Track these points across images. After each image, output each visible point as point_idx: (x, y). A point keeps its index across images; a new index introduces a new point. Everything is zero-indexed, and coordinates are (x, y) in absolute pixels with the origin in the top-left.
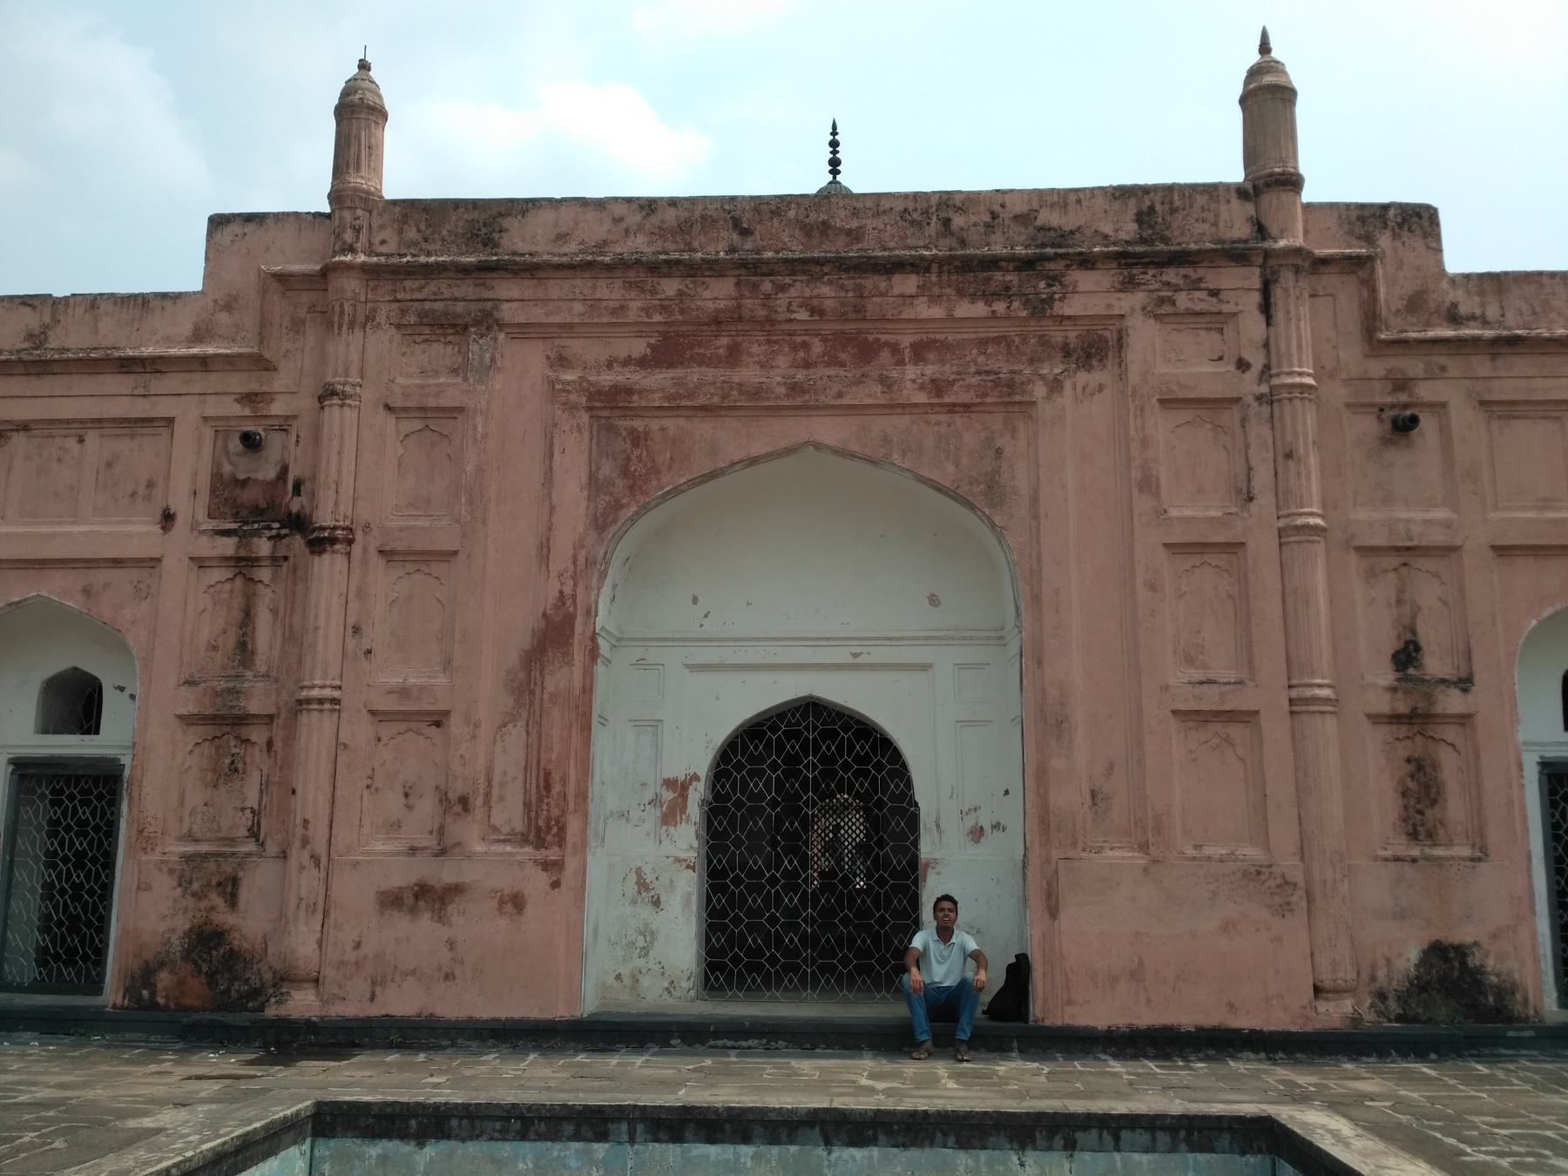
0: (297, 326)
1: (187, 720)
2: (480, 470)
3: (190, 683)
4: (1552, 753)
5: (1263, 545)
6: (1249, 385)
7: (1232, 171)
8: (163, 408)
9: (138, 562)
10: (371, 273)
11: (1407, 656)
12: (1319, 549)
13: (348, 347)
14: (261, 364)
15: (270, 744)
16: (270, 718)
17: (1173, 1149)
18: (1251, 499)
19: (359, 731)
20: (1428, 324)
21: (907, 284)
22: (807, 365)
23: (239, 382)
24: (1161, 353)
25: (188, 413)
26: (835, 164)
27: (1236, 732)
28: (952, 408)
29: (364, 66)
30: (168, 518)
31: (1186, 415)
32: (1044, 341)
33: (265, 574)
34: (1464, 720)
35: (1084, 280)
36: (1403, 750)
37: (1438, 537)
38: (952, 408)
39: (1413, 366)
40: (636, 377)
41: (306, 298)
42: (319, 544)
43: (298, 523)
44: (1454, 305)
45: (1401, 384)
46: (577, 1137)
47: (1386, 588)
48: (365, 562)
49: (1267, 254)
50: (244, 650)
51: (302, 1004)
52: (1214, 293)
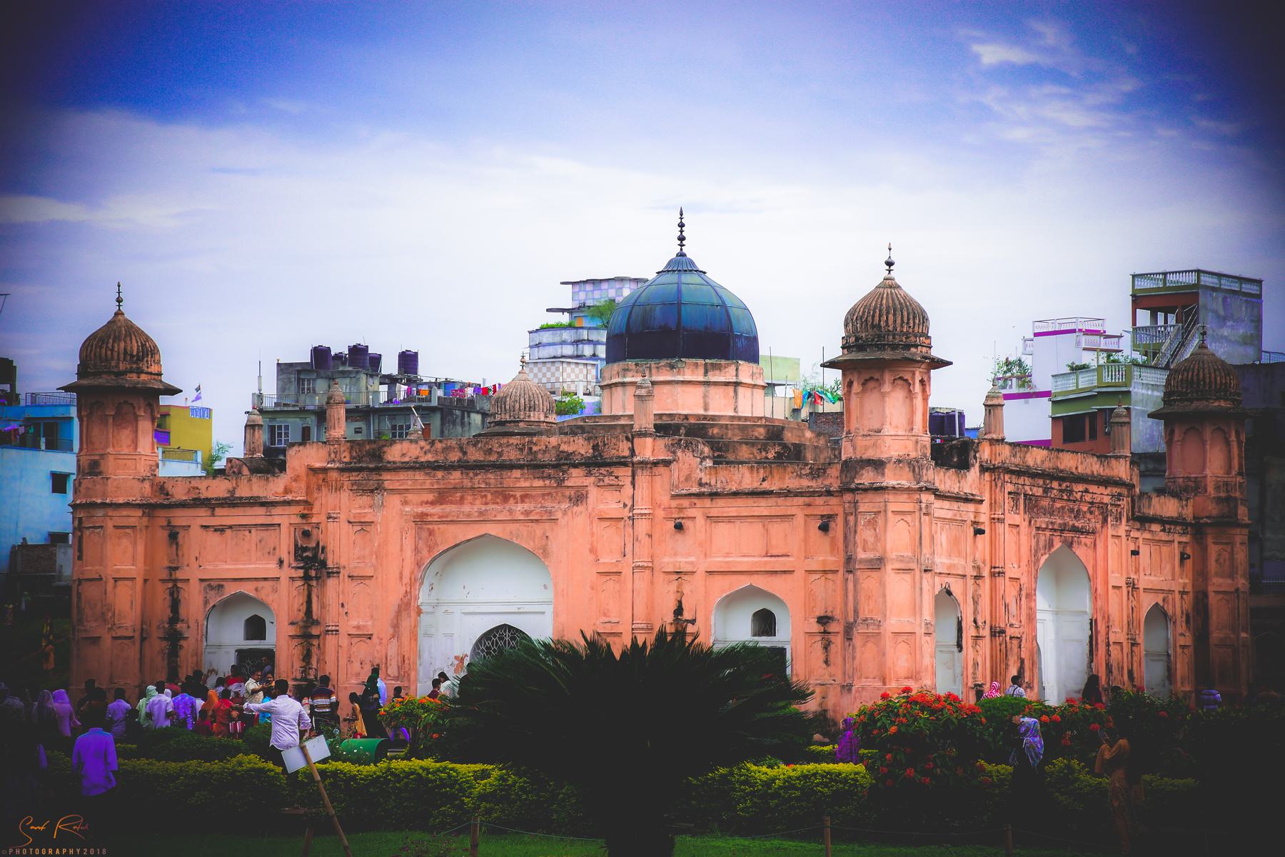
0: (319, 488)
1: (292, 637)
3: (292, 624)
5: (627, 572)
6: (626, 513)
8: (276, 520)
9: (273, 579)
10: (341, 470)
11: (679, 611)
16: (318, 637)
19: (344, 641)
25: (284, 521)
26: (682, 239)
28: (532, 521)
30: (281, 562)
31: (607, 523)
33: (314, 583)
35: (574, 472)
38: (532, 521)
39: (685, 502)
40: (430, 510)
41: (321, 476)
42: (329, 575)
43: (323, 564)
45: (681, 509)
47: (673, 587)
50: (309, 611)
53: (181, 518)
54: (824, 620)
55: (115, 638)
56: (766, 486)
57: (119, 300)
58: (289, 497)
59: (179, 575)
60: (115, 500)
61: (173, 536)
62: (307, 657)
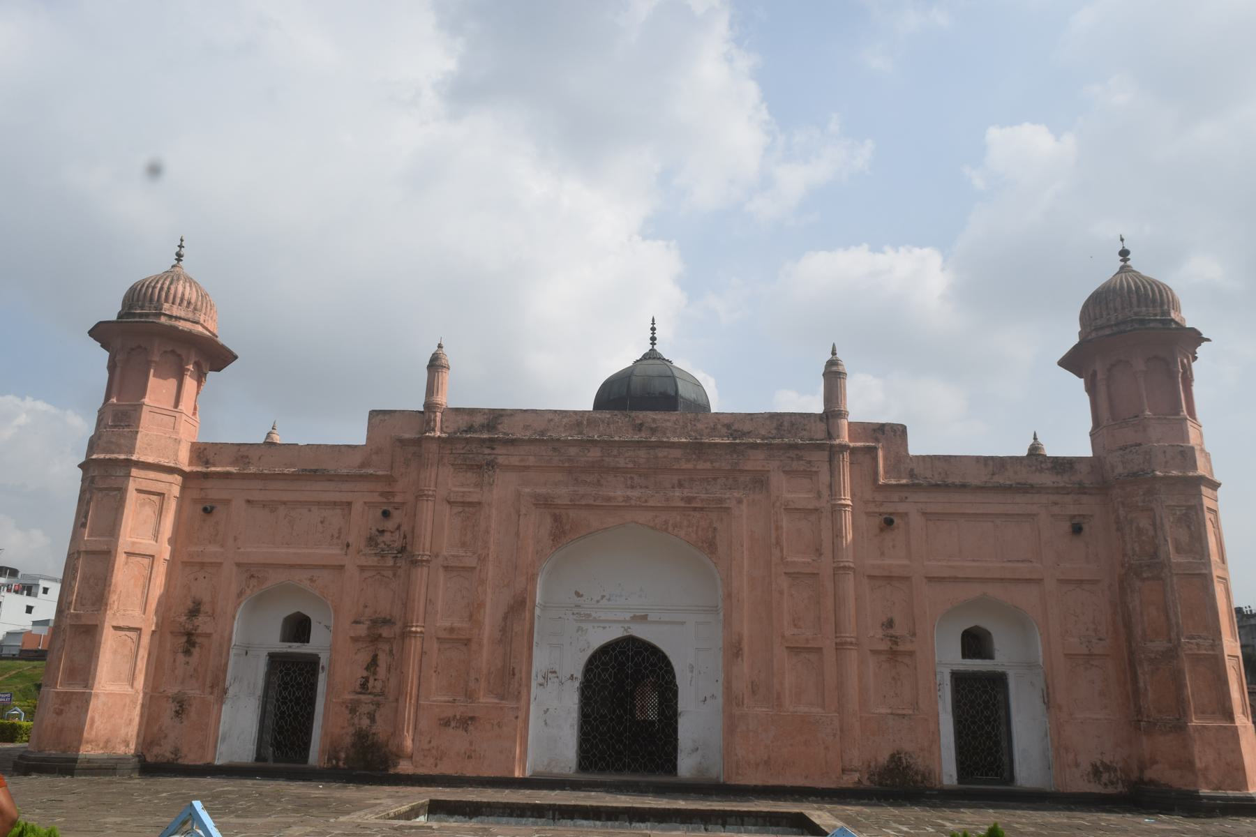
1: (355, 639)
4: (955, 668)
7: (817, 407)
12: (851, 576)
14: (390, 480)
15: (391, 651)
17: (764, 825)
18: (821, 555)
20: (900, 478)
26: (653, 339)
28: (695, 509)
29: (440, 346)
34: (911, 654)
38: (695, 509)
42: (414, 562)
44: (912, 470)
46: (532, 816)
49: (832, 446)
51: (404, 767)
52: (809, 462)
56: (999, 479)
57: (179, 257)
58: (371, 471)
60: (142, 459)
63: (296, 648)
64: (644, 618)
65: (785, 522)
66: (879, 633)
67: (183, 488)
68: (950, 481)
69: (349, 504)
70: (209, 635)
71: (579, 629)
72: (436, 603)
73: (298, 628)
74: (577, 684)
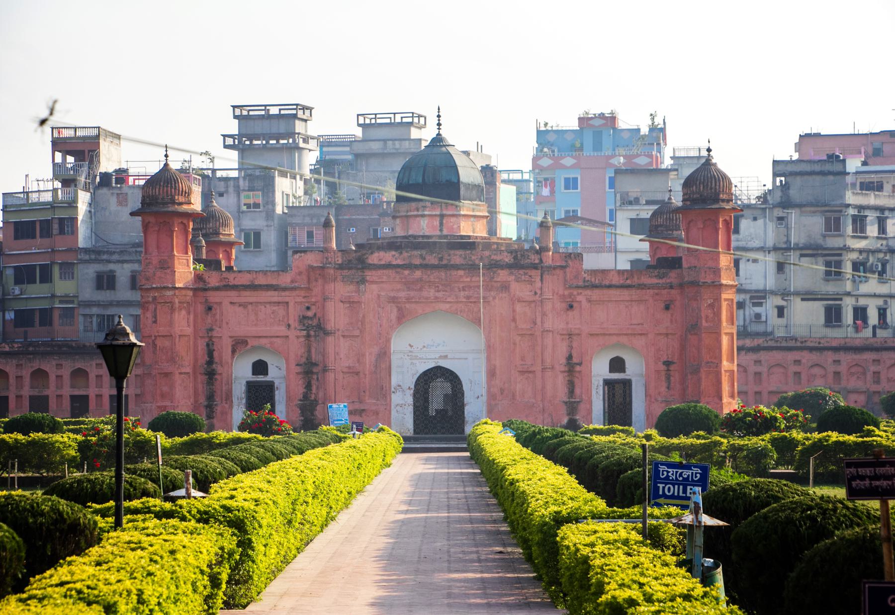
2: (364, 316)
3: (297, 365)
8: (287, 299)
11: (570, 357)
13: (331, 286)
15: (318, 379)
16: (317, 373)
21: (461, 273)
22: (438, 291)
23: (303, 293)
24: (521, 290)
26: (439, 124)
27: (531, 375)
32: (492, 286)
33: (313, 339)
34: (580, 372)
36: (567, 378)
37: (577, 332)
39: (575, 293)
42: (327, 333)
48: (339, 339)
53: (214, 297)
54: (668, 363)
55: (181, 373)
56: (629, 282)
59: (215, 334)
61: (210, 309)
62: (308, 386)
63: (261, 378)
64: (446, 357)
65: (519, 308)
66: (564, 361)
67: (194, 295)
68: (604, 283)
69: (287, 303)
70: (221, 374)
71: (412, 363)
72: (339, 352)
73: (260, 367)
74: (412, 391)
